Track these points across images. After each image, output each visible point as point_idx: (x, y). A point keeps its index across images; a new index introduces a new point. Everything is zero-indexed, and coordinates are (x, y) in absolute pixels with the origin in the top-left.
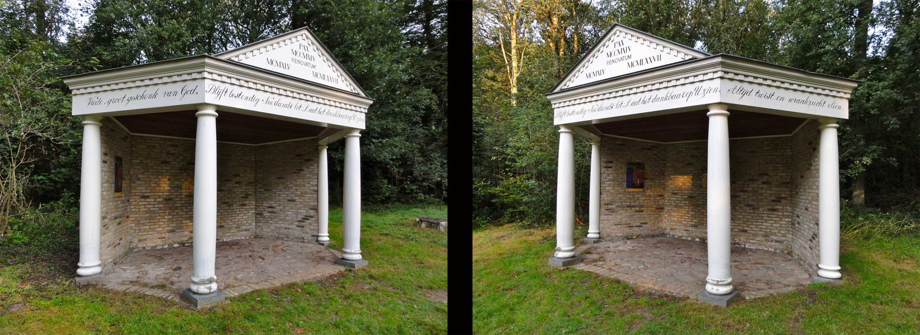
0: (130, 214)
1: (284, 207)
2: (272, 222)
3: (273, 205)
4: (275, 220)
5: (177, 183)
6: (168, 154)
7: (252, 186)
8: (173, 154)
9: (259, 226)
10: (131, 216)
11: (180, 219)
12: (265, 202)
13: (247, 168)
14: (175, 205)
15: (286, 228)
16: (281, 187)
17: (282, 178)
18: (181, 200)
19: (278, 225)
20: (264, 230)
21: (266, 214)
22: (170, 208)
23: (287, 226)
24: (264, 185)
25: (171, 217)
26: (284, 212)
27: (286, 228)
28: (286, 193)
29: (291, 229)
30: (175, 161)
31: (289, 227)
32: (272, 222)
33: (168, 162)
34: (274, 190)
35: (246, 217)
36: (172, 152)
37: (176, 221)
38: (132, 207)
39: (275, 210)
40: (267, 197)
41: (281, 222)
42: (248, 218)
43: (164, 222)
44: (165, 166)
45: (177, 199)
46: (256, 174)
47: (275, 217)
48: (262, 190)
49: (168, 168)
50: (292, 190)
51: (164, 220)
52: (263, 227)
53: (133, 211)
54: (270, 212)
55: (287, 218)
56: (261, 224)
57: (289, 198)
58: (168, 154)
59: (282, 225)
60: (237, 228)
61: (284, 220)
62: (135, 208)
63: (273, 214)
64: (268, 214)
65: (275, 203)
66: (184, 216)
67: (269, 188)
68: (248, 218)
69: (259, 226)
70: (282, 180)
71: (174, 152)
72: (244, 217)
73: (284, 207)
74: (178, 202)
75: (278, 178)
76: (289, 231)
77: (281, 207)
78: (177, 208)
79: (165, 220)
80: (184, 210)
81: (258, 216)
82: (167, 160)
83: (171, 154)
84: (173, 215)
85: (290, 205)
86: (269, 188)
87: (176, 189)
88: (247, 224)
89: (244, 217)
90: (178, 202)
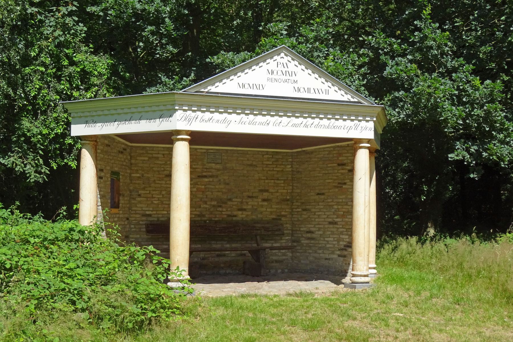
0: (130, 234)
1: (324, 232)
3: (313, 229)
7: (288, 205)
9: (296, 258)
10: (131, 236)
12: (303, 226)
15: (326, 259)
20: (302, 261)
26: (324, 238)
28: (327, 213)
29: (332, 259)
39: (314, 236)
41: (321, 251)
48: (300, 210)
54: (309, 239)
56: (298, 254)
57: (330, 220)
63: (312, 242)
64: (306, 242)
65: (314, 227)
67: (307, 207)
75: (318, 194)
76: (330, 262)
77: (321, 233)
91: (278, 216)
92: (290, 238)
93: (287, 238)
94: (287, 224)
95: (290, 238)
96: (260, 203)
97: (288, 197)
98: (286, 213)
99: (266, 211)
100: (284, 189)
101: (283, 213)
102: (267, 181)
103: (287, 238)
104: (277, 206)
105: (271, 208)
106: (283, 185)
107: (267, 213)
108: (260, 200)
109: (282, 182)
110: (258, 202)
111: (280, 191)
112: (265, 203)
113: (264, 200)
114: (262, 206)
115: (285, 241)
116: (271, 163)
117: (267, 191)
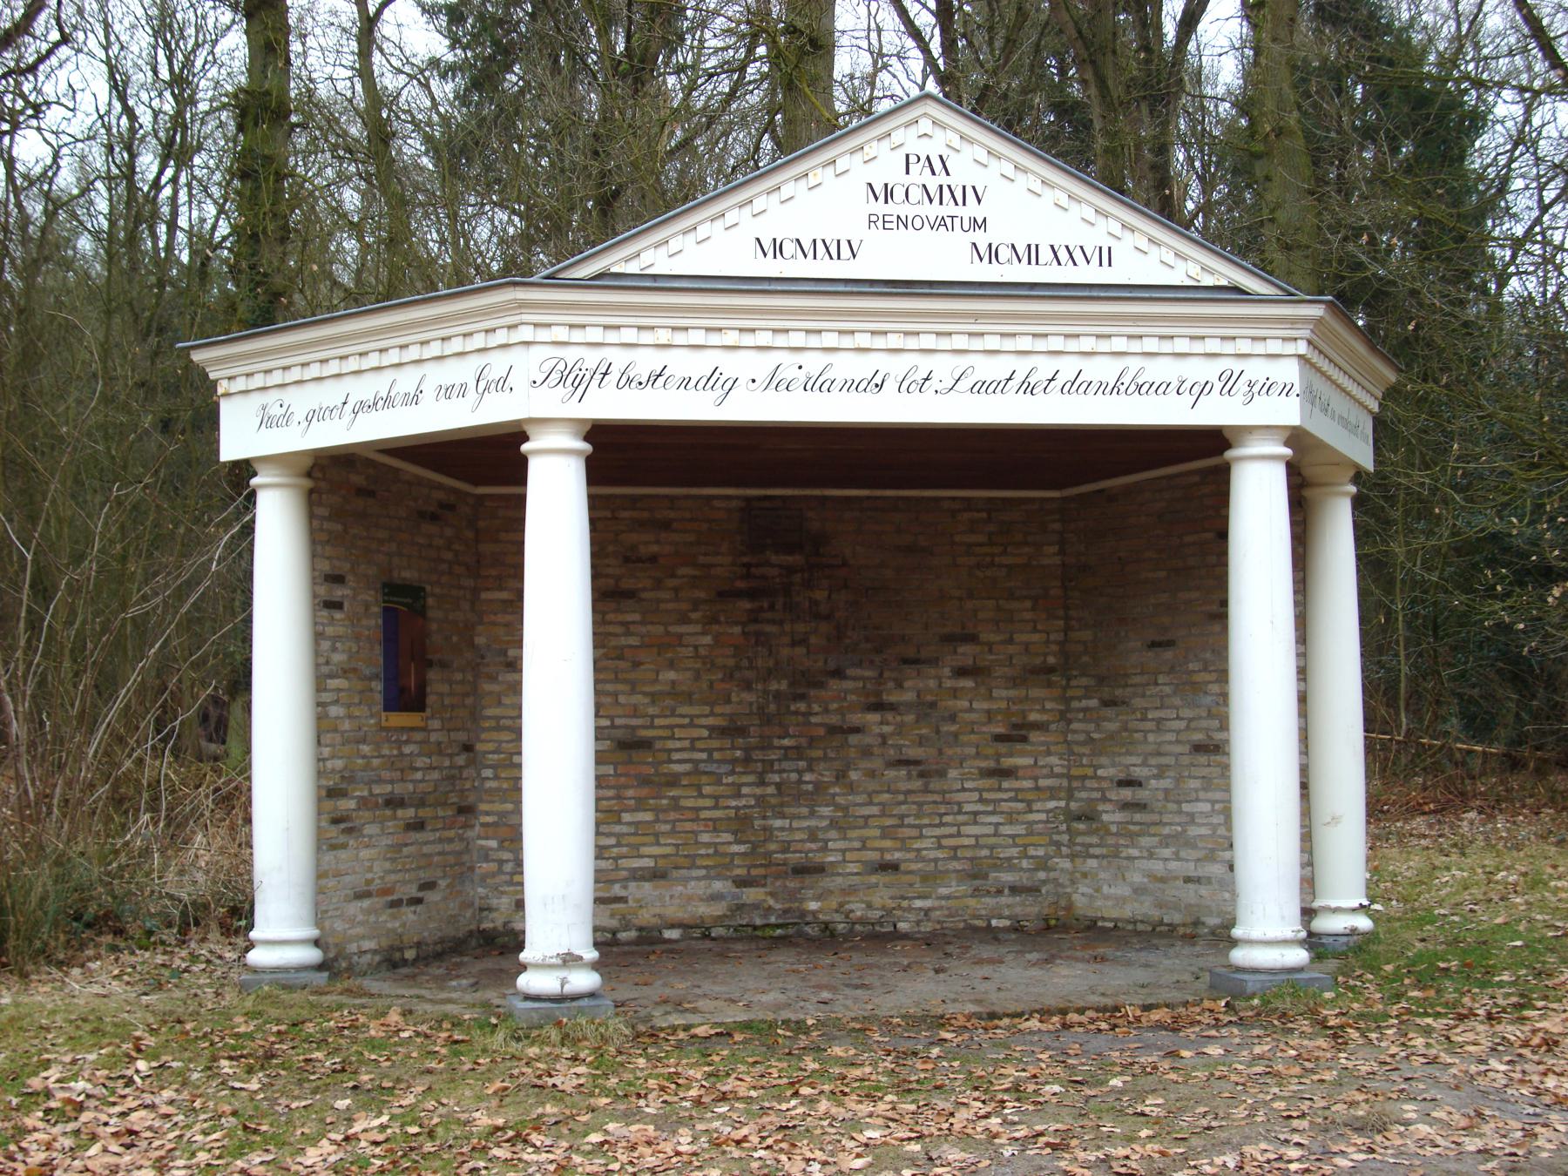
0: (481, 801)
1: (1179, 780)
2: (1134, 852)
3: (1139, 772)
4: (1145, 841)
5: (671, 675)
6: (627, 560)
7: (1049, 685)
8: (653, 559)
9: (1085, 875)
10: (483, 807)
11: (688, 826)
12: (1104, 760)
13: (1015, 605)
14: (665, 768)
15: (1188, 880)
16: (1165, 685)
17: (1170, 644)
18: (693, 749)
19: (1157, 867)
20: (1105, 889)
21: (1111, 817)
22: (645, 781)
23: (1190, 869)
24: (1101, 680)
25: (648, 816)
26: (1179, 803)
27: (1188, 880)
28: (1187, 713)
29: (1209, 880)
30: (658, 584)
31: (1200, 873)
32: (1134, 852)
33: (630, 594)
34: (1138, 702)
35: (1019, 829)
36: (644, 551)
37: (673, 832)
38: (488, 773)
39: (1142, 795)
40: (1112, 736)
41: (1167, 852)
42: (1030, 833)
43: (619, 836)
44: (617, 611)
45: (671, 744)
46: (1067, 630)
47: (1146, 826)
48: (1093, 703)
49: (629, 617)
50: (1208, 700)
51: (617, 829)
52: (1102, 875)
53: (491, 790)
54: (1126, 806)
55: (1193, 831)
56: (1092, 863)
57: (1198, 737)
58: (627, 560)
59: (1173, 865)
60: (975, 877)
61: (1179, 840)
62: (496, 777)
63: (1138, 817)
64: (1119, 817)
65: (1144, 764)
66: (704, 814)
67: (1119, 692)
68: (1030, 833)
69: (1085, 875)
70: (1168, 655)
71: (655, 548)
72: (1007, 830)
73: (1179, 780)
74: (676, 756)
75: (1154, 645)
76: (1204, 891)
77: (1166, 783)
78: (673, 781)
79: (625, 829)
80: (707, 790)
81: (1081, 826)
82: (627, 584)
83: (640, 560)
84: (657, 810)
85: (1205, 771)
86: (1119, 692)
87: (668, 702)
88: (1025, 864)
89: (1007, 830)
90: (676, 756)
91: (1015, 726)
92: (1062, 804)
93: (1052, 804)
94: (1049, 753)
95: (1062, 804)
96: (948, 684)
97: (1051, 660)
98: (1045, 717)
99: (971, 710)
100: (1035, 630)
101: (1034, 717)
102: (969, 605)
103: (1052, 804)
104: (1012, 693)
105: (990, 697)
106: (1028, 616)
107: (973, 716)
108: (947, 671)
109: (1028, 604)
110: (939, 678)
111: (1018, 637)
112: (968, 683)
113: (961, 672)
114: (955, 693)
115: (1043, 816)
116: (981, 538)
117: (972, 639)
